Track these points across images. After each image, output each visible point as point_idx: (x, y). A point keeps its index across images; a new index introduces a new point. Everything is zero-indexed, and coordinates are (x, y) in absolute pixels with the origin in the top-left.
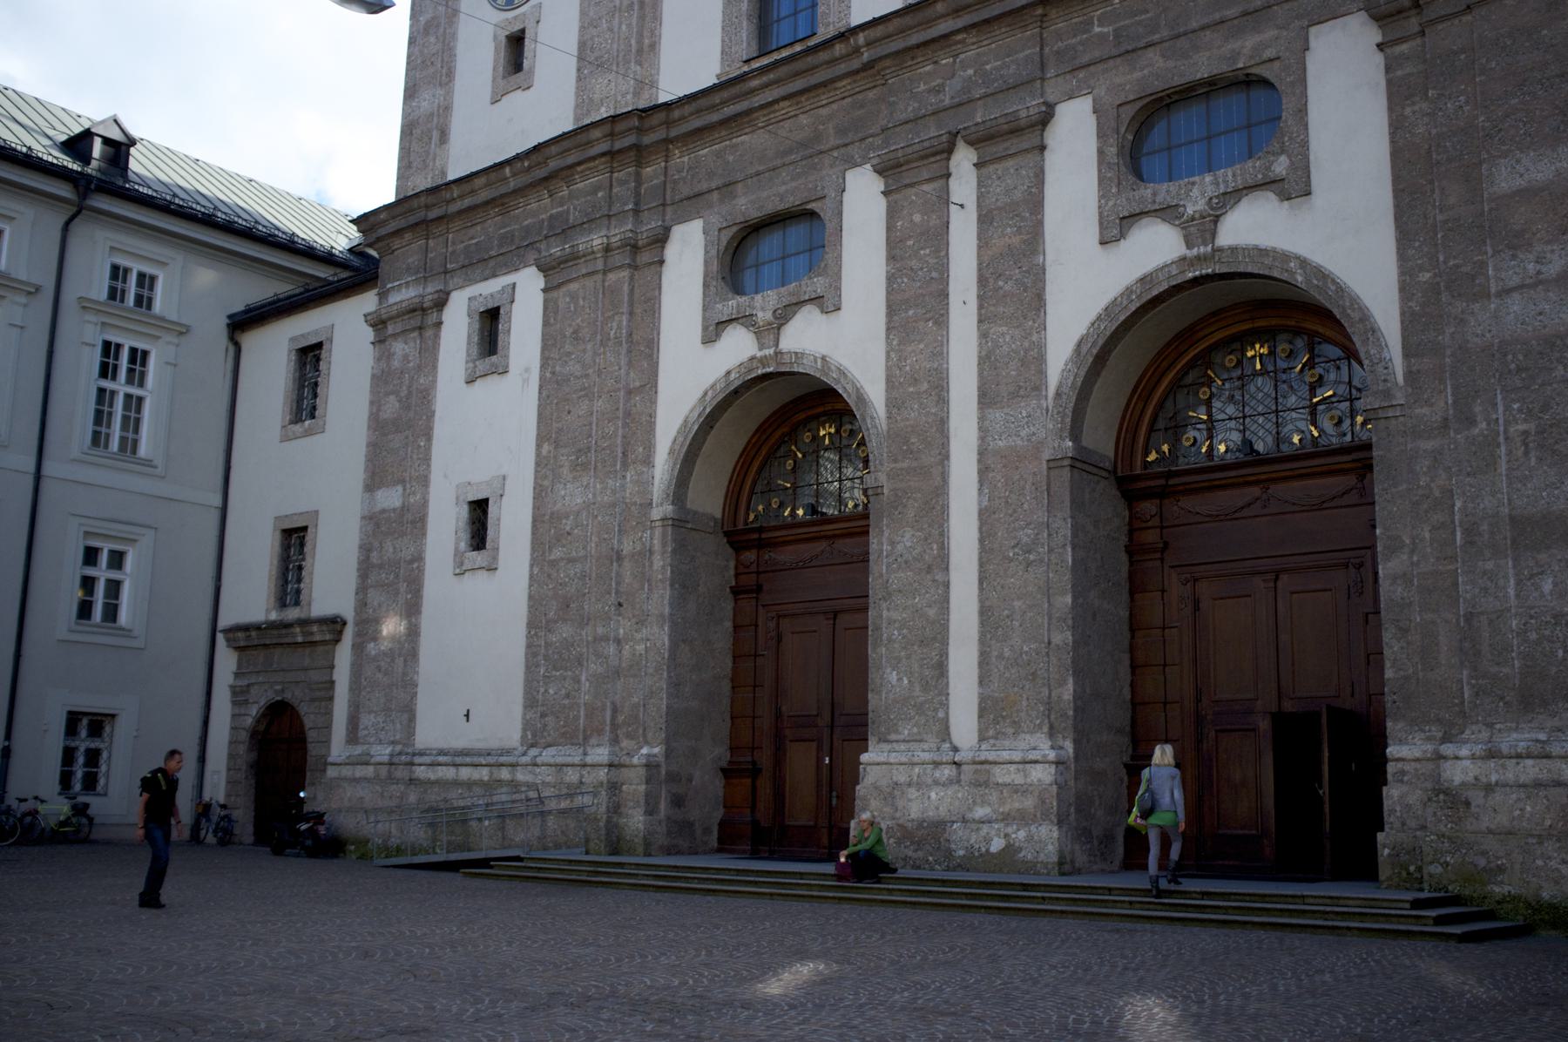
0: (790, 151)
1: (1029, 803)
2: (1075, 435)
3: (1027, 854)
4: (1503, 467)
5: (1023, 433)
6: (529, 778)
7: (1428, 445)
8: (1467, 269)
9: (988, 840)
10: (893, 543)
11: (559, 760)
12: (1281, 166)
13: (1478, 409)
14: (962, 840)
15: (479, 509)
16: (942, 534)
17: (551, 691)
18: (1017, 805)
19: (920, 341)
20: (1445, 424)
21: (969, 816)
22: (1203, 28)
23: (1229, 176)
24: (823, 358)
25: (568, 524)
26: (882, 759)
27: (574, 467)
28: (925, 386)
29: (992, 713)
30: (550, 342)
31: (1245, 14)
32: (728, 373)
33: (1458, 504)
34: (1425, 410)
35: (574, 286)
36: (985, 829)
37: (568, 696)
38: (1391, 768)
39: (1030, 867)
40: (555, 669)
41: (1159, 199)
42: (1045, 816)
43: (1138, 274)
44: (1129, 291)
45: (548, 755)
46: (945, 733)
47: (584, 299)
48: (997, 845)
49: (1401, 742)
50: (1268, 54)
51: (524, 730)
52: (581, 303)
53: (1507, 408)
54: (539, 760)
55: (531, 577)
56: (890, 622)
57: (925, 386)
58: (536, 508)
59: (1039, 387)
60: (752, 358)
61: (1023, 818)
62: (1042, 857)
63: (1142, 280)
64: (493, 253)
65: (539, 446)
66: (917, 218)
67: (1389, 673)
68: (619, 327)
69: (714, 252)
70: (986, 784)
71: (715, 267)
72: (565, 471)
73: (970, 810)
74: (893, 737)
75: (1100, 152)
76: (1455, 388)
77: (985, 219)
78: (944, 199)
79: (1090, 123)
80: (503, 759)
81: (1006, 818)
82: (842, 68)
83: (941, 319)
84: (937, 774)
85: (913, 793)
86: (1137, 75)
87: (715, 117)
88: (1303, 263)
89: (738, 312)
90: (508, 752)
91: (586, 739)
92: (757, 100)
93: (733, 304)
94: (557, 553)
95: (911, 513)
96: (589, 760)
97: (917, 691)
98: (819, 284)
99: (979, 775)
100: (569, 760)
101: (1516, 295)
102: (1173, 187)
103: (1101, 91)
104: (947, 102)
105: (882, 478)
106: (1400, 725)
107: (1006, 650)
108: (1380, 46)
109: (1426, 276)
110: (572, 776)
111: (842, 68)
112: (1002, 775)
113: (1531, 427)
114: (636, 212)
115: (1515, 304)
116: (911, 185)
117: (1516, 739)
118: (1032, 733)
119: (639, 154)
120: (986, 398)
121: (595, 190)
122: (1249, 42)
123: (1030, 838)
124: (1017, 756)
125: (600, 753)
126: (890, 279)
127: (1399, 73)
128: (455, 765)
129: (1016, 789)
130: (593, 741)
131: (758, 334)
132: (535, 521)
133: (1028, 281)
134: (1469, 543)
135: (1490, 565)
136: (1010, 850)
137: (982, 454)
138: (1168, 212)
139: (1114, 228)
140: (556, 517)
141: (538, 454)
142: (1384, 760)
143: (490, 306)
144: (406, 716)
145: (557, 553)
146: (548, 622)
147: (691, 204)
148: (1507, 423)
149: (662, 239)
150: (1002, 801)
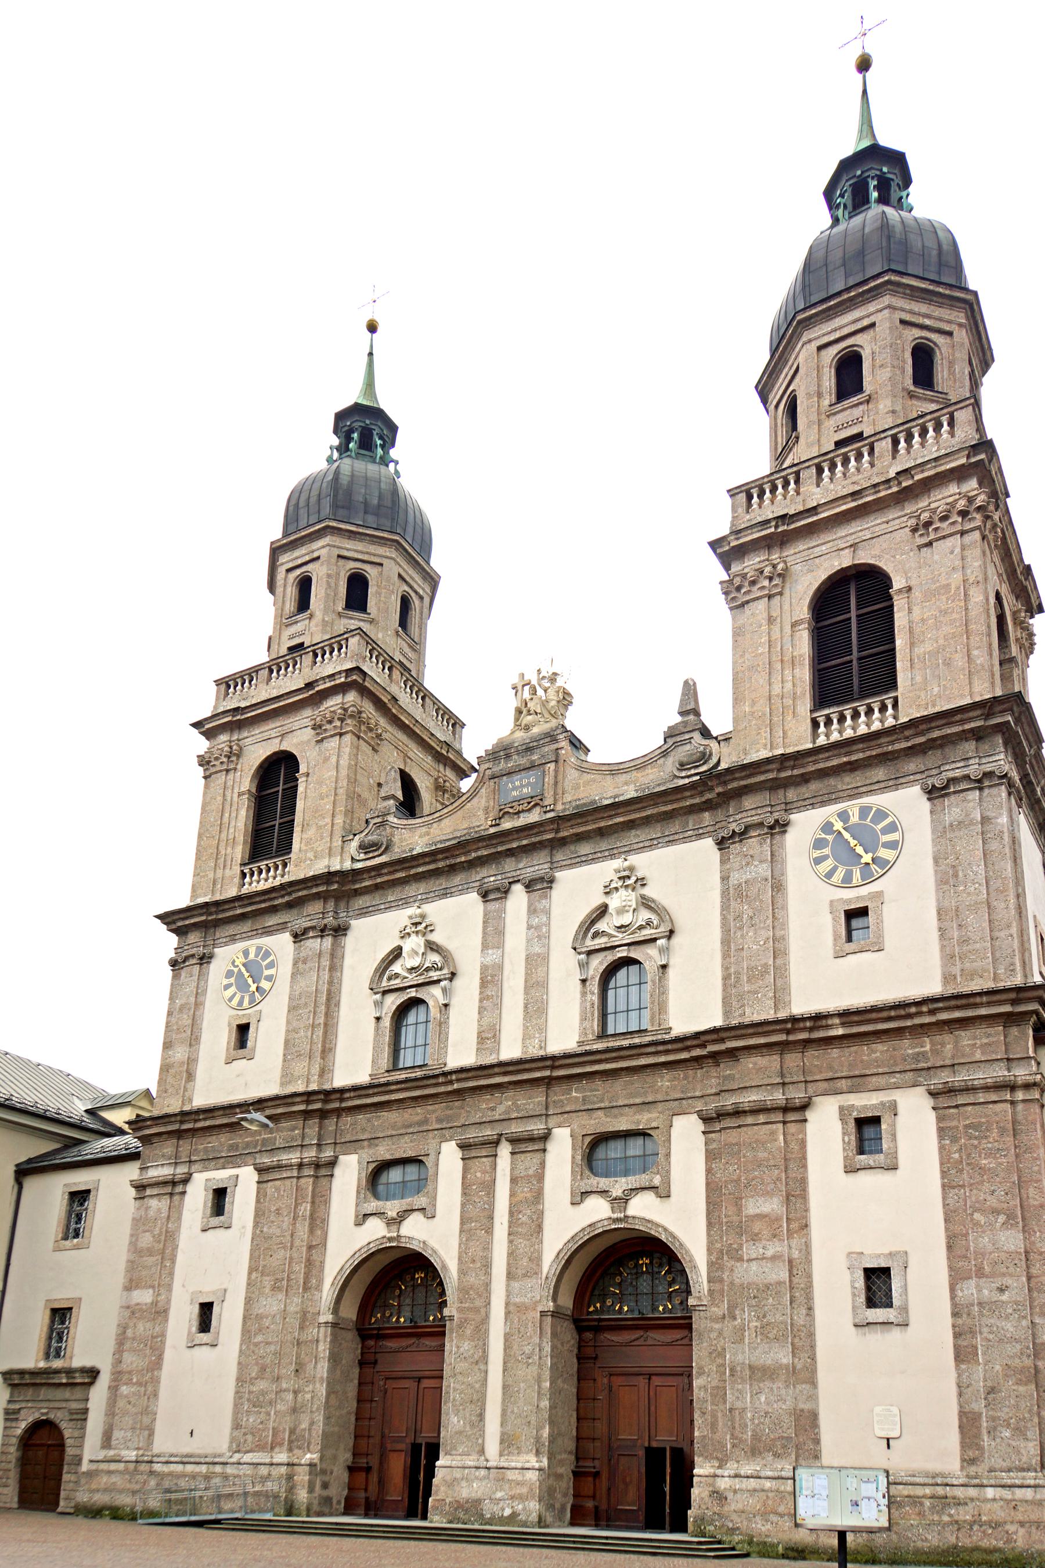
2: (554, 1299)
3: (523, 1517)
4: (747, 1341)
6: (235, 1472)
7: (717, 1326)
8: (735, 1246)
11: (255, 1461)
13: (737, 1312)
15: (206, 1309)
17: (251, 1420)
25: (267, 1322)
27: (274, 1288)
33: (728, 1357)
34: (716, 1309)
35: (278, 1183)
37: (262, 1423)
38: (695, 1479)
39: (525, 1524)
40: (254, 1406)
45: (248, 1458)
49: (701, 1467)
51: (231, 1443)
53: (749, 1314)
54: (242, 1461)
55: (241, 1351)
58: (246, 1310)
62: (530, 1519)
65: (250, 1273)
67: (696, 1434)
68: (305, 1210)
69: (364, 1175)
71: (364, 1182)
72: (267, 1290)
76: (729, 1301)
80: (217, 1460)
90: (219, 1456)
91: (272, 1448)
94: (259, 1338)
96: (275, 1461)
100: (263, 1461)
101: (754, 1262)
106: (701, 1459)
108: (704, 1133)
109: (718, 1245)
110: (264, 1471)
113: (758, 1324)
114: (319, 1145)
115: (754, 1266)
123: (524, 1509)
125: (282, 1457)
130: (277, 1450)
131: (388, 1224)
132: (245, 1318)
134: (732, 1375)
135: (740, 1387)
136: (514, 1515)
139: (580, 1197)
140: (260, 1317)
141: (249, 1278)
142: (692, 1476)
145: (259, 1338)
146: (251, 1379)
147: (354, 1144)
148: (749, 1322)
149: (332, 1163)
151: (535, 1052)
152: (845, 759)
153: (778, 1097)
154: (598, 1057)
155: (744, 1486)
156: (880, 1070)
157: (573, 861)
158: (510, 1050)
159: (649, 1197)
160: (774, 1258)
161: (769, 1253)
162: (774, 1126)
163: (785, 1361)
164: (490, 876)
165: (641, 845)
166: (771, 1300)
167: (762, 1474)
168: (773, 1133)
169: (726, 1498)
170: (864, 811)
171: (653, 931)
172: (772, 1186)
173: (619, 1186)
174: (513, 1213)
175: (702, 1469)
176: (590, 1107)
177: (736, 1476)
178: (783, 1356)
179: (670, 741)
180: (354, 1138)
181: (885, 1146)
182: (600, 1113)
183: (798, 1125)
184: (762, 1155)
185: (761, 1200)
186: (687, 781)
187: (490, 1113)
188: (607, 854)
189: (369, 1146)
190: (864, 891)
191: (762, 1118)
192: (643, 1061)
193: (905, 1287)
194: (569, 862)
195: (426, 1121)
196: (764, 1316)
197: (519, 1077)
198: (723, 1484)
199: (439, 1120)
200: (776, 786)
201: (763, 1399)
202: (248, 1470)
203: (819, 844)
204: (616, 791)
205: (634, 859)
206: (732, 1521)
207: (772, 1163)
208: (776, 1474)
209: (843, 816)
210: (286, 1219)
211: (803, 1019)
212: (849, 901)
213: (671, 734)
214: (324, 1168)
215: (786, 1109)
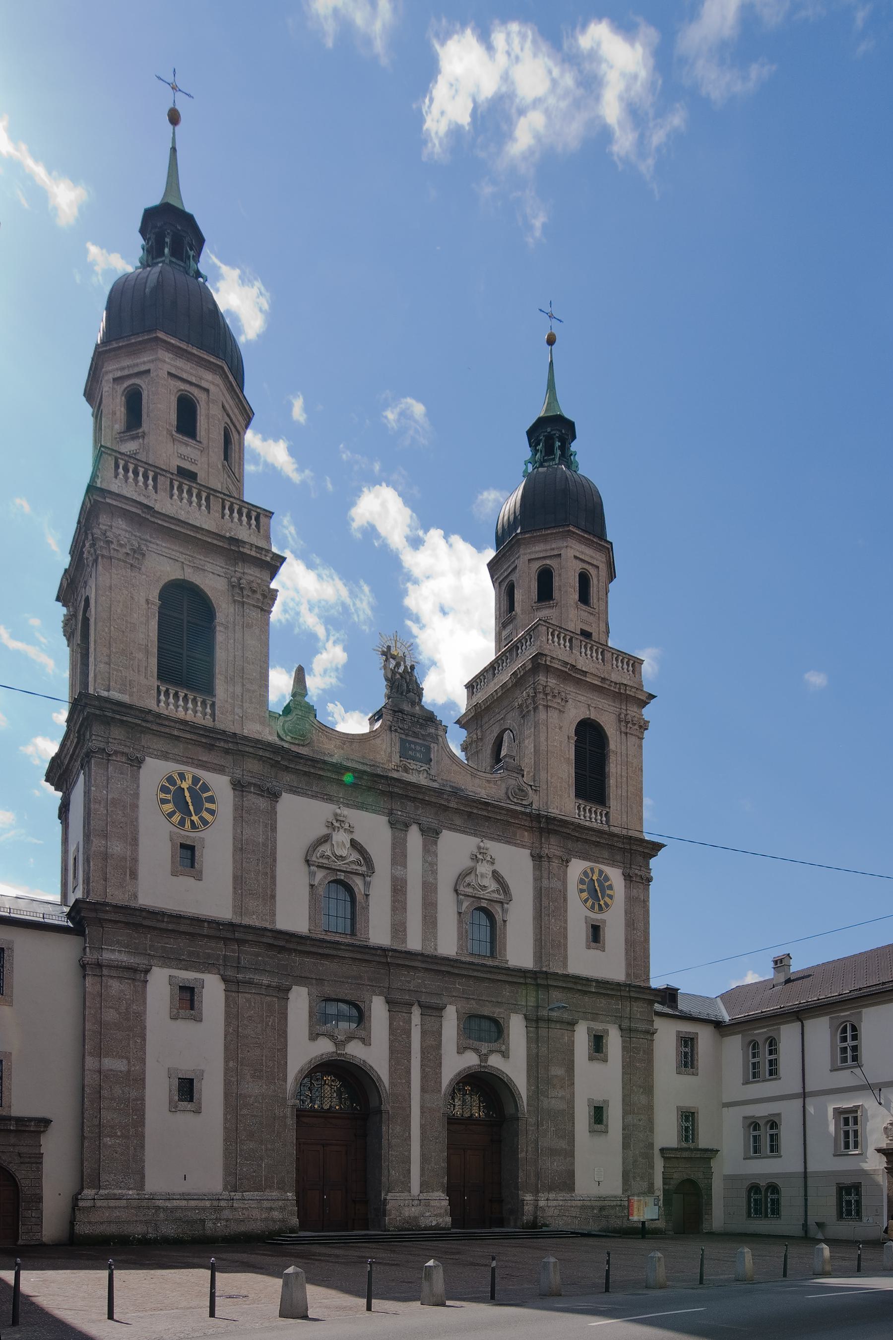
5: (436, 1104)
10: (393, 1130)
12: (503, 1048)
14: (423, 1222)
16: (410, 1130)
18: (439, 1212)
19: (402, 1066)
22: (487, 1001)
28: (404, 1081)
29: (425, 1186)
32: (323, 1055)
42: (447, 1215)
43: (467, 1065)
46: (409, 1191)
47: (255, 1003)
48: (434, 1223)
50: (502, 1016)
52: (253, 1004)
56: (392, 1155)
57: (404, 1081)
59: (440, 1091)
60: (334, 1052)
63: (468, 1068)
66: (401, 1023)
73: (424, 1213)
74: (393, 1191)
75: (458, 1025)
77: (424, 1033)
78: (409, 1022)
79: (455, 1016)
81: (436, 1215)
82: (377, 959)
84: (413, 1203)
85: (407, 1209)
87: (320, 951)
88: (507, 1075)
89: (327, 1032)
92: (340, 953)
95: (399, 1121)
97: (401, 1177)
98: (363, 1034)
102: (478, 1043)
104: (412, 988)
105: (389, 1108)
107: (430, 1168)
111: (377, 959)
116: (400, 1012)
117: (552, 1196)
118: (437, 1191)
119: (281, 949)
120: (423, 1090)
121: (257, 955)
122: (498, 1010)
126: (391, 1042)
127: (530, 1035)
137: (422, 1107)
138: (476, 1050)
147: (302, 980)
150: (434, 1210)
151: (429, 951)
153: (566, 1016)
154: (476, 968)
158: (414, 943)
160: (562, 1098)
161: (560, 1095)
162: (563, 1031)
163: (564, 1147)
165: (493, 836)
171: (498, 896)
192: (499, 977)
197: (431, 967)
204: (474, 789)
205: (488, 844)
210: (259, 1025)
214: (283, 992)
215: (568, 1023)
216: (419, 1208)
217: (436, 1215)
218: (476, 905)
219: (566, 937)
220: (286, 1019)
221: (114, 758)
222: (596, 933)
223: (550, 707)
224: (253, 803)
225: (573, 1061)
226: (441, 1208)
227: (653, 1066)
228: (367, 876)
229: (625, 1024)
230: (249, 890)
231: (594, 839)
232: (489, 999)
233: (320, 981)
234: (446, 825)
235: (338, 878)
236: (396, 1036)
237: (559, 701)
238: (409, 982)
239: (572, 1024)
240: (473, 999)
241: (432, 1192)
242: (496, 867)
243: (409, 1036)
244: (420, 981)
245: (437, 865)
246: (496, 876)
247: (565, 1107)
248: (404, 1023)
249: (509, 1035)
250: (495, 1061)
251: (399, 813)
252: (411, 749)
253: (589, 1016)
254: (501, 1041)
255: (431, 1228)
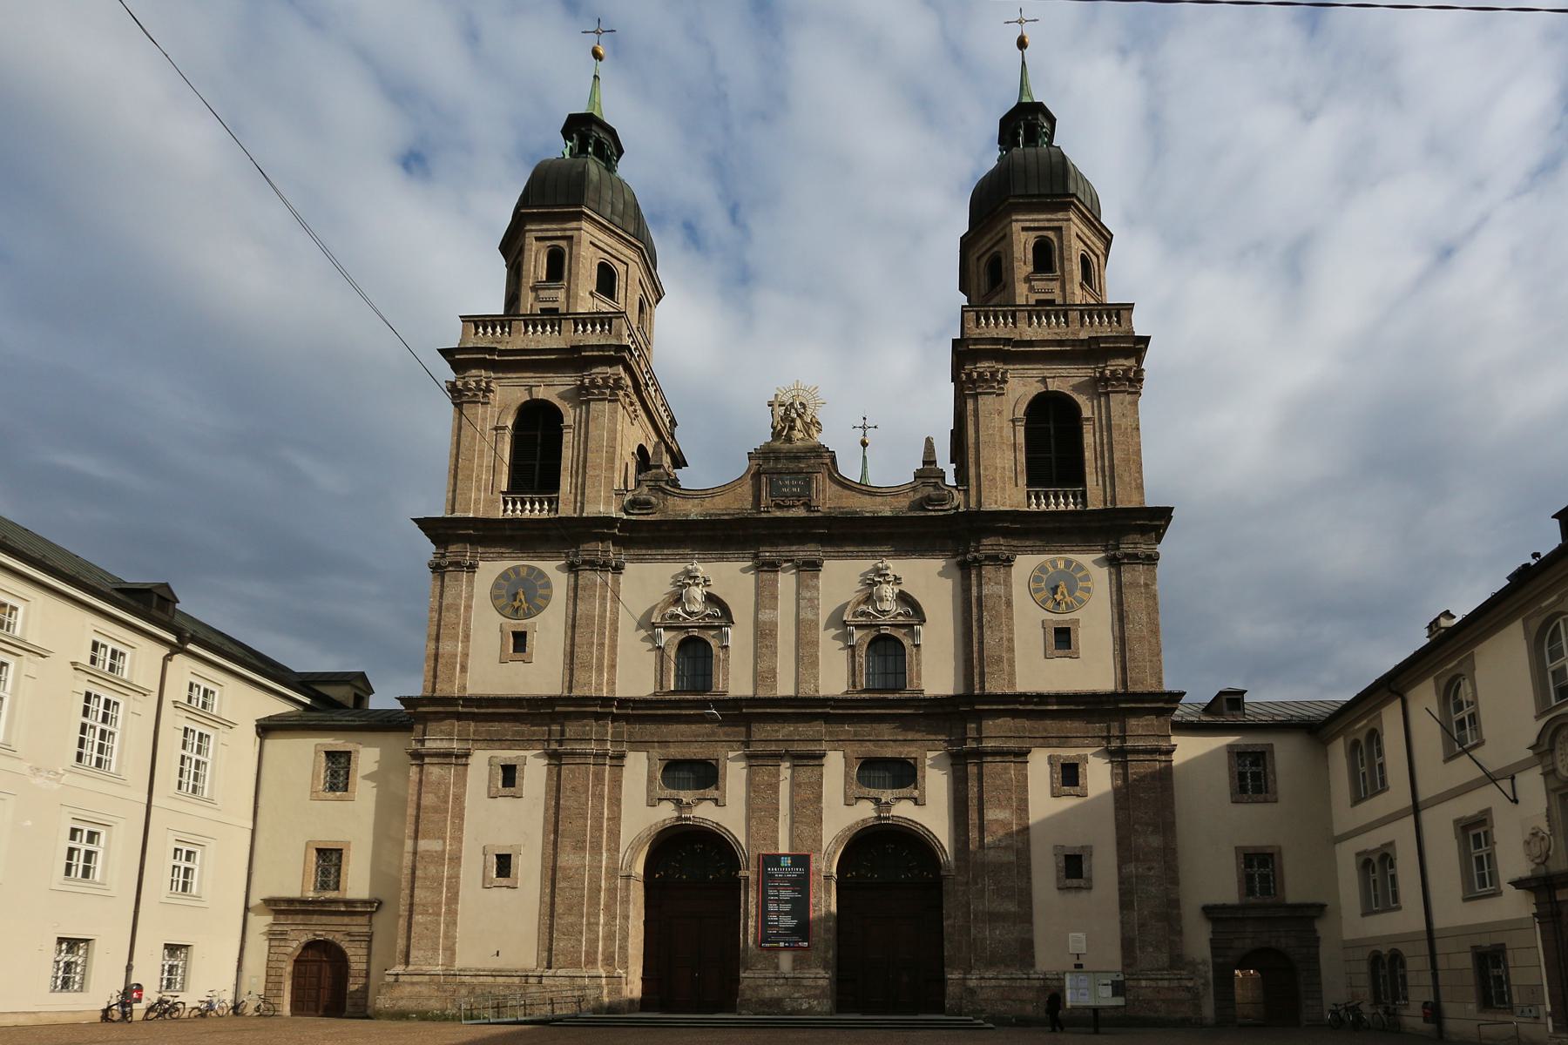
0: (699, 736)
1: (818, 992)
6: (552, 983)
7: (963, 888)
9: (801, 1004)
12: (916, 793)
18: (812, 993)
20: (967, 883)
21: (792, 996)
22: (889, 740)
23: (898, 792)
24: (717, 824)
26: (752, 976)
30: (556, 790)
31: (905, 740)
33: (972, 907)
36: (800, 1001)
41: (871, 794)
44: (857, 823)
47: (579, 774)
48: (805, 1006)
50: (913, 755)
52: (577, 775)
59: (820, 850)
61: (816, 997)
64: (508, 738)
67: (946, 954)
70: (799, 985)
75: (846, 774)
81: (808, 997)
83: (777, 820)
85: (766, 989)
86: (863, 749)
93: (668, 792)
98: (716, 794)
99: (796, 983)
103: (848, 751)
104: (780, 737)
108: (952, 765)
109: (963, 838)
112: (805, 982)
124: (813, 976)
128: (492, 976)
129: (812, 987)
133: (817, 812)
135: (981, 925)
136: (811, 1007)
143: (509, 763)
144: (448, 953)
149: (621, 757)
152: (1058, 525)
153: (1012, 744)
155: (987, 985)
156: (1079, 735)
157: (840, 554)
159: (910, 804)
163: (1013, 909)
164: (767, 554)
166: (1004, 874)
167: (1000, 977)
168: (1006, 769)
169: (975, 992)
170: (1068, 563)
172: (1006, 802)
173: (886, 795)
174: (793, 807)
175: (953, 976)
176: (861, 739)
177: (981, 978)
178: (1012, 907)
179: (920, 481)
180: (642, 740)
181: (1080, 782)
182: (868, 743)
183: (1023, 765)
184: (999, 782)
185: (997, 811)
186: (933, 513)
187: (774, 734)
188: (869, 554)
189: (659, 748)
190: (1067, 617)
191: (998, 759)
193: (1090, 866)
194: (836, 554)
195: (714, 734)
196: (999, 883)
198: (972, 983)
199: (726, 734)
200: (1007, 533)
201: (998, 933)
202: (566, 982)
203: (1037, 579)
206: (980, 1006)
207: (1006, 787)
208: (1008, 977)
209: (1054, 563)
211: (1032, 696)
212: (1058, 622)
213: (919, 475)
215: (1016, 754)
216: (784, 988)
217: (808, 997)
218: (873, 633)
219: (1011, 650)
220: (620, 786)
221: (450, 569)
222: (1063, 638)
223: (981, 394)
224: (589, 579)
225: (1026, 800)
226: (816, 987)
227: (1172, 794)
228: (725, 626)
229: (1115, 744)
230: (581, 663)
231: (1051, 525)
232: (894, 738)
233: (664, 743)
234: (832, 554)
235: (690, 634)
236: (758, 792)
237: (995, 384)
238: (777, 731)
239: (1021, 755)
240: (870, 741)
241: (809, 968)
242: (902, 588)
243: (776, 792)
244: (792, 729)
245: (818, 599)
246: (903, 598)
247: (1013, 858)
248: (768, 776)
249: (924, 777)
250: (904, 810)
251: (768, 554)
252: (786, 486)
253: (1055, 741)
254: (913, 786)
255: (799, 1012)
